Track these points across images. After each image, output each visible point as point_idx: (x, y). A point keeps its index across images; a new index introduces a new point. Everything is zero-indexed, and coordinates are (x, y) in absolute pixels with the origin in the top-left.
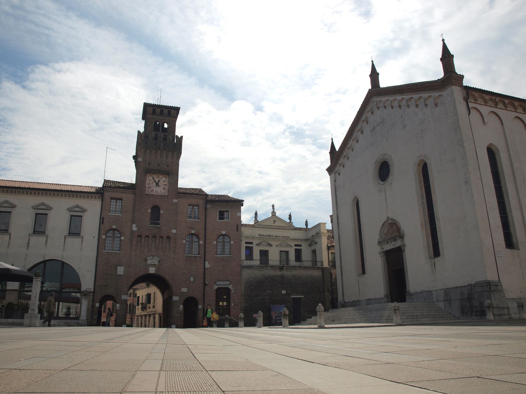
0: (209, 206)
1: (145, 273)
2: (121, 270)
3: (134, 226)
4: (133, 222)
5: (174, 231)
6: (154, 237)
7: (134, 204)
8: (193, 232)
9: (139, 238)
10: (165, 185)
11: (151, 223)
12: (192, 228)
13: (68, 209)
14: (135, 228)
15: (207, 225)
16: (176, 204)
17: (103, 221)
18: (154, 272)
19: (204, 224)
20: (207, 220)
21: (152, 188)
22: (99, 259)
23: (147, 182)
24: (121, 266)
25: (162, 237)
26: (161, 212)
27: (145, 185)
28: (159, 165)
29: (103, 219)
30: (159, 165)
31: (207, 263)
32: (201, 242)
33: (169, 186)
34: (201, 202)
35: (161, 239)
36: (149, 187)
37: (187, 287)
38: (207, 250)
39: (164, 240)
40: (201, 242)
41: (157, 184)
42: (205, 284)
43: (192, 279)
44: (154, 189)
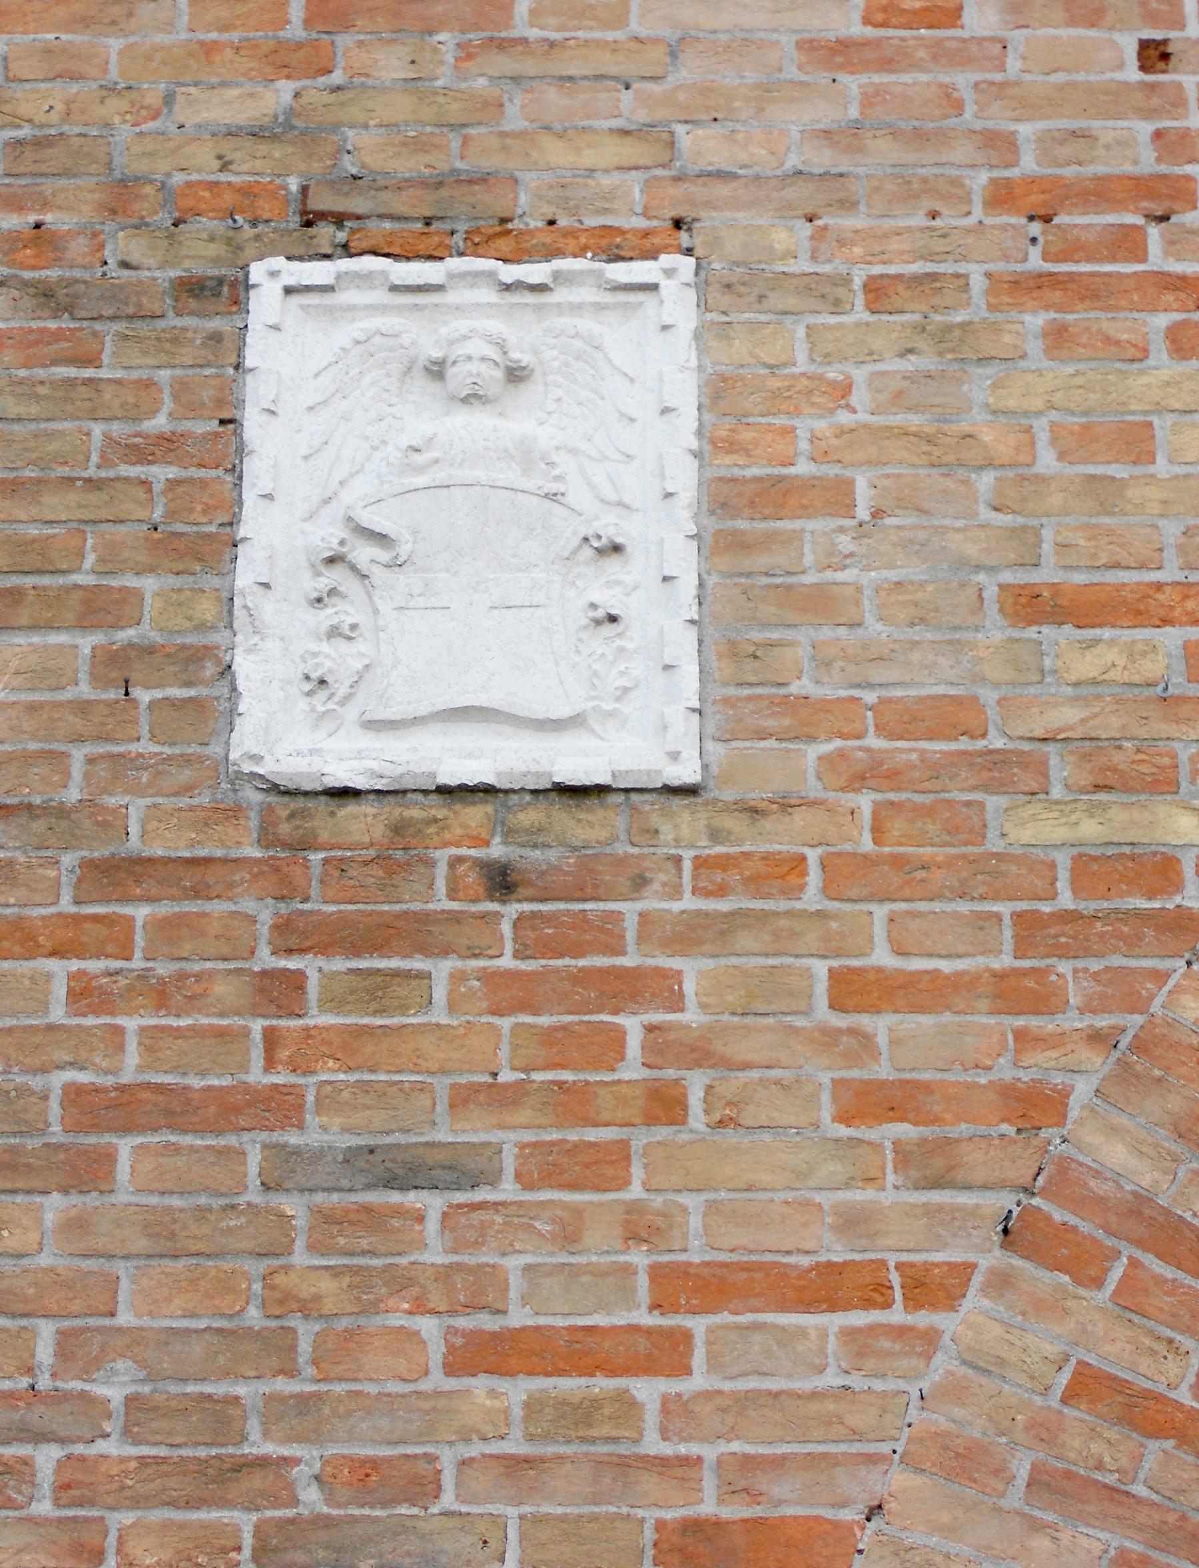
24: (448, 217)
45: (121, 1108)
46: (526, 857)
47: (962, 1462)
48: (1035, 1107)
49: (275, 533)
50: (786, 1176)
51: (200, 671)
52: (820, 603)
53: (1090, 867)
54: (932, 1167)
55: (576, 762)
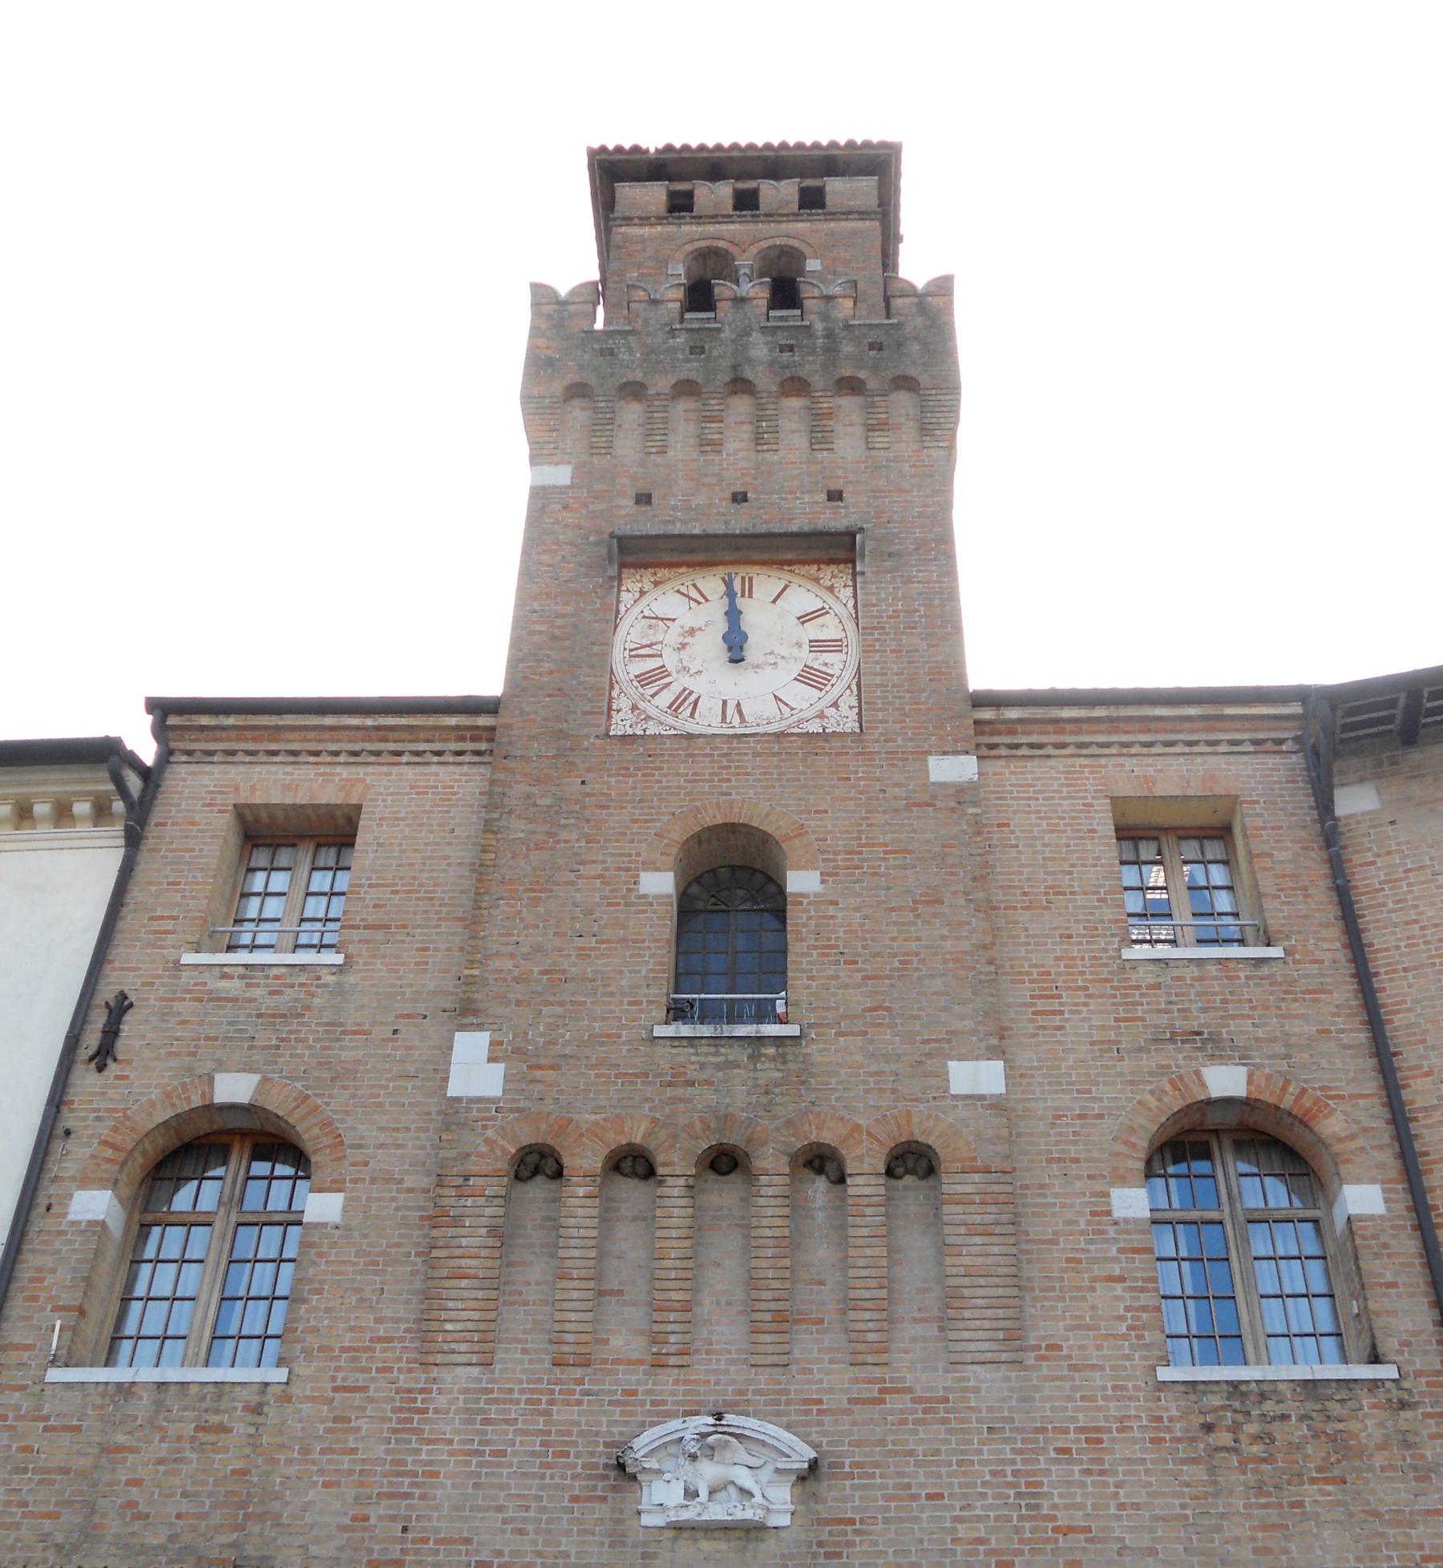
0: (1355, 801)
4: (467, 1014)
5: (977, 1076)
6: (725, 1161)
7: (488, 827)
8: (1225, 1081)
9: (538, 1189)
10: (817, 646)
11: (678, 1012)
14: (474, 1069)
15: (1391, 990)
16: (962, 794)
19: (1345, 992)
20: (1380, 938)
23: (630, 631)
25: (820, 1161)
26: (800, 882)
27: (600, 660)
30: (739, 498)
32: (1363, 1198)
33: (867, 650)
35: (819, 1188)
36: (644, 679)
39: (866, 1182)
40: (1363, 1198)
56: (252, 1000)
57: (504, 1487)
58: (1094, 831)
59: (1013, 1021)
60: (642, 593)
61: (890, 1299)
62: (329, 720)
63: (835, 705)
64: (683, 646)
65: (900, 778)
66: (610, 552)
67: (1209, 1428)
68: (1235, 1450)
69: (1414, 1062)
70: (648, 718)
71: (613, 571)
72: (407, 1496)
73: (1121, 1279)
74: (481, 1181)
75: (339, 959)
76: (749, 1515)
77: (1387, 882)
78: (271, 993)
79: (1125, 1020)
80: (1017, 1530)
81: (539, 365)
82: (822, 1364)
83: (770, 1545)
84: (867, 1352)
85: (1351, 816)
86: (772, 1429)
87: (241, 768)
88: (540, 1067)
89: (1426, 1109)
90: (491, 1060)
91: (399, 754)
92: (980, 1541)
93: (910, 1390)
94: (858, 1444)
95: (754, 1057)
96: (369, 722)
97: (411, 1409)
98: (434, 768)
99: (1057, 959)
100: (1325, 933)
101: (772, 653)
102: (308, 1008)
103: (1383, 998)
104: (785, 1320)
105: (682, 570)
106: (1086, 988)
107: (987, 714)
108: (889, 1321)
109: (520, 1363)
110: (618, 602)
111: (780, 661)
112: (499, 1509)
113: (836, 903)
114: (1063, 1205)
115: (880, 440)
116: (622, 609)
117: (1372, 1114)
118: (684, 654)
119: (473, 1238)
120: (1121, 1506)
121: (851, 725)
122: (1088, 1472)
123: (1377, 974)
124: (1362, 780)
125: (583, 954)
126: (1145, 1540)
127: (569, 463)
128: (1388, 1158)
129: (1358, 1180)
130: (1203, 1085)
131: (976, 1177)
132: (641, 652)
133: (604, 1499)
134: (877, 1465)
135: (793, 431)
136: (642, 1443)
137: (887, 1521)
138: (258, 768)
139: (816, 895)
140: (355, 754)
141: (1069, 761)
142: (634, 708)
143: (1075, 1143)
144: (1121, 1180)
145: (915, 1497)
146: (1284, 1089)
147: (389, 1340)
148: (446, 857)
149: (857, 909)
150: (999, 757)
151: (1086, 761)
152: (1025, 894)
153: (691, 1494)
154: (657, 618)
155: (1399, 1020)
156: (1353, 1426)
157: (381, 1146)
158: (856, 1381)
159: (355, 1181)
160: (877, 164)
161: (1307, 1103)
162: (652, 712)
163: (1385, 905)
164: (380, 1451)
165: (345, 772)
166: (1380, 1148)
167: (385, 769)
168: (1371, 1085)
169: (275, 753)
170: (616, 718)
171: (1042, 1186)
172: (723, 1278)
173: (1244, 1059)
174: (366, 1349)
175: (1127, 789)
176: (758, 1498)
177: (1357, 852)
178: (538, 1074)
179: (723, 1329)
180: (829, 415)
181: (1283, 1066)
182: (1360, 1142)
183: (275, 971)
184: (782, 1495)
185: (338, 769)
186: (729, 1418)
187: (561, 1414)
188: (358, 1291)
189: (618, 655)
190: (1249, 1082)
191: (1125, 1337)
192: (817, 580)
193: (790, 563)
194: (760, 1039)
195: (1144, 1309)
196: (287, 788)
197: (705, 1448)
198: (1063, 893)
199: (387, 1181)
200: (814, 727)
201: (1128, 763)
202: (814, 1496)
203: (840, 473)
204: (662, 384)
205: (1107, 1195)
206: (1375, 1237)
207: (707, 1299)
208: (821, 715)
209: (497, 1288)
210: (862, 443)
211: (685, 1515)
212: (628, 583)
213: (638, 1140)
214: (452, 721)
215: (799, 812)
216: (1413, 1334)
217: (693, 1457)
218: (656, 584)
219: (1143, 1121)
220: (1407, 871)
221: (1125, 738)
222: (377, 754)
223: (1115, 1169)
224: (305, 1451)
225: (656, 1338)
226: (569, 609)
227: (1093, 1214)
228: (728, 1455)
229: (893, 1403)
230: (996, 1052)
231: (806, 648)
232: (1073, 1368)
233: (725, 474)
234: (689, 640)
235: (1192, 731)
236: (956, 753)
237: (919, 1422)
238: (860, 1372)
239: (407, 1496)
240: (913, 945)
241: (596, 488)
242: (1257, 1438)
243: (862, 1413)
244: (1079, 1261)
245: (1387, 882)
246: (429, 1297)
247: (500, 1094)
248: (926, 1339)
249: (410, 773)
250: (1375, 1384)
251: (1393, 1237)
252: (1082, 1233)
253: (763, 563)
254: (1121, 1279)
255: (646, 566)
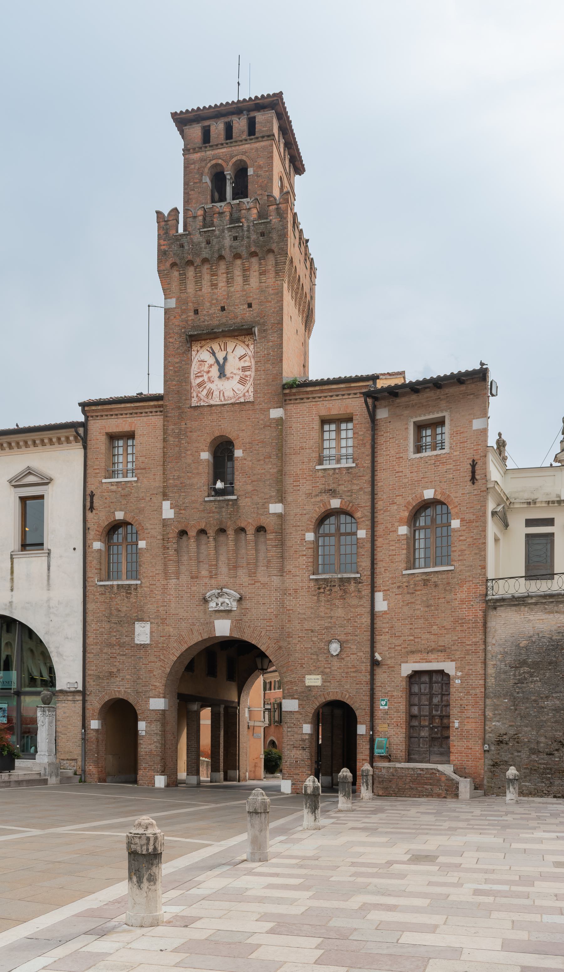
0: (382, 414)
1: (205, 636)
2: (143, 633)
3: (166, 505)
4: (165, 496)
5: (276, 508)
7: (165, 440)
9: (184, 538)
10: (244, 369)
12: (333, 493)
13: (10, 481)
17: (92, 502)
18: (227, 634)
19: (368, 477)
20: (380, 459)
21: (209, 385)
22: (90, 606)
23: (195, 368)
24: (141, 620)
26: (238, 453)
28: (223, 309)
29: (92, 495)
31: (379, 596)
32: (362, 534)
33: (257, 370)
34: (356, 405)
36: (200, 385)
37: (323, 673)
38: (380, 555)
41: (222, 374)
42: (375, 663)
43: (335, 648)
44: (213, 386)
45: (132, 656)
46: (143, 646)
47: (157, 668)
48: (160, 656)
49: (136, 634)
50: (152, 658)
51: (133, 639)
52: (154, 636)
53: (162, 647)
54: (156, 658)
55: (146, 643)
56: (119, 492)
57: (183, 604)
58: (313, 428)
59: (288, 489)
60: (198, 351)
61: (257, 562)
62: (123, 405)
63: (248, 391)
64: (208, 372)
65: (262, 417)
66: (187, 339)
67: (319, 588)
68: (324, 593)
69: (380, 496)
70: (201, 399)
71: (188, 345)
72: (166, 606)
73: (305, 555)
74: (172, 539)
75: (135, 479)
76: (228, 608)
77: (385, 442)
78: (123, 489)
79: (314, 487)
80: (279, 610)
81: (162, 254)
82: (243, 576)
83: (233, 614)
84: (252, 574)
85: (381, 419)
86: (232, 592)
87: (105, 420)
88: (181, 510)
89: (380, 510)
90: (171, 508)
91: (141, 413)
92: (272, 612)
93: (260, 582)
94: (250, 593)
95: (227, 505)
96: (132, 405)
97: (165, 588)
98: (150, 417)
99: (300, 470)
100: (367, 458)
101: (232, 373)
102: (131, 493)
103: (376, 478)
104: (235, 567)
105: (208, 341)
106: (306, 478)
107: (287, 391)
108: (256, 566)
109: (184, 578)
110: (191, 355)
111: (234, 376)
112: (183, 608)
113: (245, 459)
114: (295, 538)
115: (263, 279)
116: (193, 358)
117: (367, 511)
118: (210, 375)
119: (171, 552)
120: (300, 605)
121: (251, 399)
122: (294, 598)
123: (377, 470)
124: (385, 407)
125: (189, 478)
126: (304, 611)
127: (174, 297)
128: (369, 523)
129: (361, 529)
130: (330, 505)
131: (274, 534)
132: (199, 375)
133: (202, 605)
134: (253, 597)
135: (238, 276)
136: (208, 594)
137: (255, 609)
138: (109, 420)
139: (241, 457)
140: (131, 414)
141: (309, 404)
142: (197, 396)
143: (299, 522)
144: (308, 531)
145: (260, 604)
146: (349, 505)
147: (158, 574)
148: (157, 447)
149: (251, 461)
150: (291, 404)
151: (314, 403)
152: (294, 450)
153: (217, 604)
154: (202, 361)
155: (379, 484)
156: (349, 587)
157: (152, 529)
158: (249, 580)
159: (147, 538)
160: (279, 95)
161: (353, 509)
162: (202, 397)
163: (383, 449)
164: (159, 597)
165: (129, 420)
166: (368, 520)
167: (139, 418)
168: (369, 504)
169: (112, 415)
170: (193, 399)
171: (291, 533)
172: (223, 558)
173: (341, 497)
174: (155, 576)
175: (324, 413)
176: (230, 605)
177: (380, 431)
178: (182, 512)
179: (223, 569)
180: (248, 270)
181: (349, 498)
182: (363, 519)
183: (123, 483)
184: (235, 604)
185: (128, 419)
186: (224, 590)
187: (194, 588)
188: (151, 563)
189: (192, 376)
190: (341, 504)
191: (304, 569)
192: (244, 342)
193: (237, 336)
194: (229, 500)
195: (309, 562)
196: (117, 426)
197: (219, 595)
198: (303, 449)
199: (154, 537)
200: (242, 400)
201: (325, 403)
202: (241, 604)
203: (251, 294)
204: (198, 261)
205: (305, 535)
206: (362, 543)
207: (220, 562)
208: (244, 395)
209: (178, 562)
210: (258, 280)
211: (216, 609)
212: (194, 348)
213: (203, 528)
214: (152, 403)
215: (238, 431)
216: (366, 566)
217: (217, 598)
218: (201, 347)
219: (315, 515)
220: (390, 438)
221: (325, 395)
222: (136, 413)
223: (307, 528)
224: (146, 597)
225: (210, 572)
226: (178, 360)
227: (301, 540)
228: (224, 597)
229: (258, 584)
230: (281, 501)
231: (241, 370)
232: (293, 576)
233: (219, 298)
234: (210, 369)
235: (343, 391)
236: (277, 408)
237: (262, 588)
238: (250, 578)
239: (166, 606)
240: (263, 471)
241: (184, 307)
242: (329, 590)
243: (250, 587)
244: (297, 551)
245: (385, 442)
246: (165, 565)
247: (173, 517)
248: (264, 570)
249: (145, 419)
250: (355, 578)
251: (366, 543)
252: (298, 544)
253: (229, 337)
254: (305, 555)
255: (198, 341)
